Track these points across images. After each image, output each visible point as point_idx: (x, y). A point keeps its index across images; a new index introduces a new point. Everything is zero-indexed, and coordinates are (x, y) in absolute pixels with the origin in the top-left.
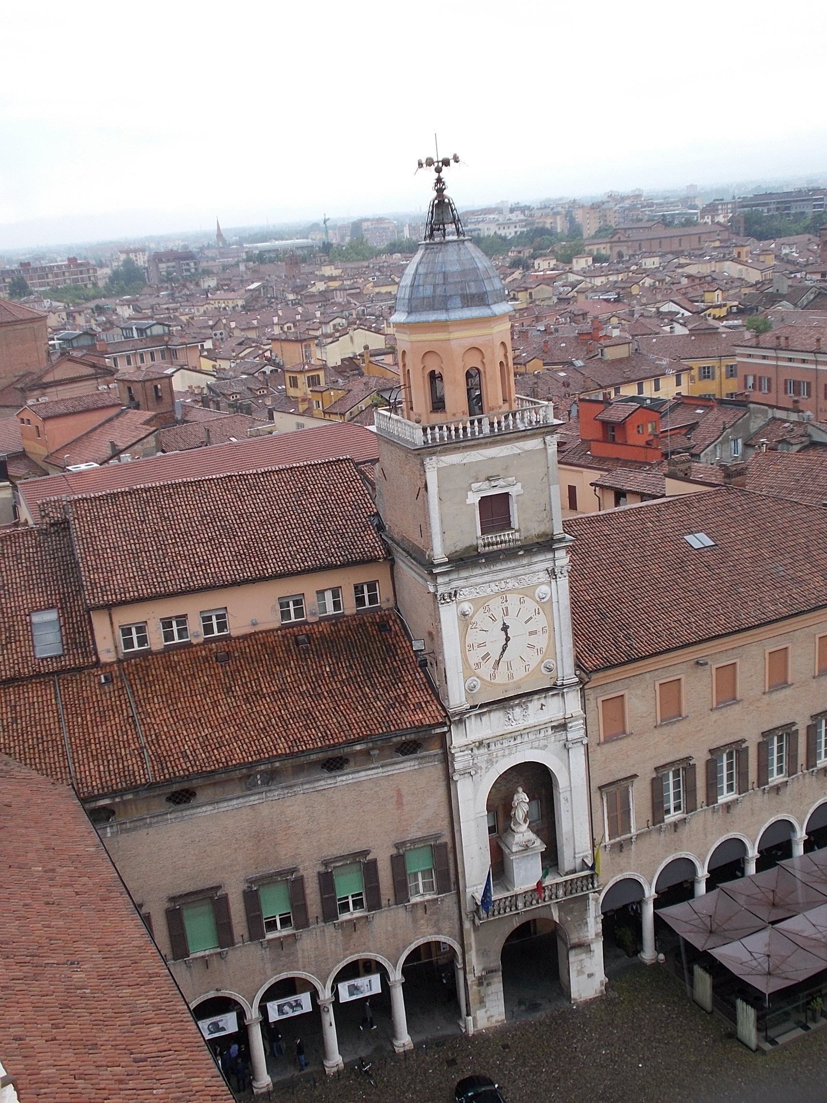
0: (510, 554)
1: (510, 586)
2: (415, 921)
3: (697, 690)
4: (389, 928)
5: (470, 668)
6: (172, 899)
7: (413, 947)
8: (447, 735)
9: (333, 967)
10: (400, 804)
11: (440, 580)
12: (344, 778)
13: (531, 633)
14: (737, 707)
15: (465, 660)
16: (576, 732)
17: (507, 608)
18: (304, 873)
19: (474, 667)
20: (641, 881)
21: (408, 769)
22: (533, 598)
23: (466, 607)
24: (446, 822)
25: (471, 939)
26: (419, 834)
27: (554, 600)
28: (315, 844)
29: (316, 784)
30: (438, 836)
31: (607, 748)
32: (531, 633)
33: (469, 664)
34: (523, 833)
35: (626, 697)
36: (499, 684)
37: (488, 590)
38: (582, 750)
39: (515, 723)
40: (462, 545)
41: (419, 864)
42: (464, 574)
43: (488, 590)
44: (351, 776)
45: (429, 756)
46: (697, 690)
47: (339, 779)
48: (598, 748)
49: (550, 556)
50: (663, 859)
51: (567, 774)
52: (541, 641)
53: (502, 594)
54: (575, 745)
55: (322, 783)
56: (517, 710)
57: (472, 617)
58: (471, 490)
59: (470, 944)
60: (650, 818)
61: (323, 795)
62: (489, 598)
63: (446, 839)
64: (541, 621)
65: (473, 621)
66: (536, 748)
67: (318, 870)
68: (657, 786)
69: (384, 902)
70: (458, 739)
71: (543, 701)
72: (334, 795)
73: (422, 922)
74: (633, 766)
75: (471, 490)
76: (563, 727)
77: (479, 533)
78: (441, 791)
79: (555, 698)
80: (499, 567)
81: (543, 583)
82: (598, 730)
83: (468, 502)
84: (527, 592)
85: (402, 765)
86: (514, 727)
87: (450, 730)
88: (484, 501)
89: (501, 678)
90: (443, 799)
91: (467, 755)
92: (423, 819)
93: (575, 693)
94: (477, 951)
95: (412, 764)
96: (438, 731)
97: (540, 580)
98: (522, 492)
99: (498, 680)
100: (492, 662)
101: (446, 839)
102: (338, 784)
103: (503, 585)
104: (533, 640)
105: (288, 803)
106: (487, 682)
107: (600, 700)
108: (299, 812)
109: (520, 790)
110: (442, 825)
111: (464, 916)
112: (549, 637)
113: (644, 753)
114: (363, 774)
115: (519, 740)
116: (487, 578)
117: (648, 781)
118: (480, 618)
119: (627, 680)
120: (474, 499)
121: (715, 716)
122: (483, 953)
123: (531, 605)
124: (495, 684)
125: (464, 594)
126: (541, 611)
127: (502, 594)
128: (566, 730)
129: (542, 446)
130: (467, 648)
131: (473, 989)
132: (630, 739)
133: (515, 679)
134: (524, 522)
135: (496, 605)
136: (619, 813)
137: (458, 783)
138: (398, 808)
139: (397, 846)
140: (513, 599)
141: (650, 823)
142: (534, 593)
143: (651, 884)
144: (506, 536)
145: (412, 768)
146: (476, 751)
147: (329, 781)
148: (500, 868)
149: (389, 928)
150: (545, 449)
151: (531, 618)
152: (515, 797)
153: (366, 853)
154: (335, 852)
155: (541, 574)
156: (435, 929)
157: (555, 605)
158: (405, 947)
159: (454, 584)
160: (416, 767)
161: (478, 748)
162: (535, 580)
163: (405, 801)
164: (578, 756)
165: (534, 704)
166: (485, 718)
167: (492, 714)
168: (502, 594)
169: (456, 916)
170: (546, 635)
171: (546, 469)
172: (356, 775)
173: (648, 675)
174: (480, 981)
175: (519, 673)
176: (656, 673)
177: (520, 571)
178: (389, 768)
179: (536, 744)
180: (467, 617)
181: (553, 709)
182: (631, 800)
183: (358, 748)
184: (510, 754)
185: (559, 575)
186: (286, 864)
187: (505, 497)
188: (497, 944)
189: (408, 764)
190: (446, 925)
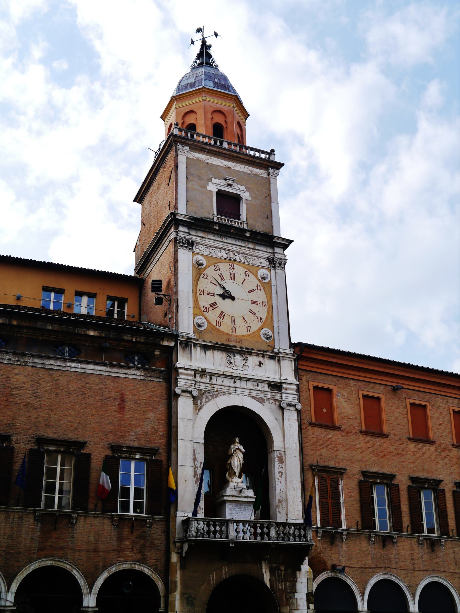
0: (239, 234)
1: (238, 258)
2: (120, 539)
3: (395, 415)
4: (92, 538)
5: (200, 308)
7: (113, 569)
8: (175, 350)
9: (24, 566)
10: (121, 408)
11: (181, 228)
12: (73, 365)
13: (253, 302)
14: (431, 448)
15: (196, 301)
16: (289, 396)
17: (234, 274)
18: (16, 446)
19: (203, 309)
20: (354, 587)
21: (134, 377)
22: (256, 276)
24: (163, 441)
26: (136, 444)
27: (273, 283)
28: (33, 420)
29: (47, 362)
30: (154, 451)
31: (317, 431)
32: (253, 302)
33: (198, 304)
34: (238, 486)
35: (334, 392)
36: (224, 333)
37: (220, 254)
38: (295, 416)
39: (235, 368)
40: (200, 215)
41: (133, 475)
42: (201, 234)
43: (220, 254)
44: (80, 365)
45: (155, 370)
46: (395, 415)
47: (69, 364)
48: (310, 428)
49: (270, 250)
51: (281, 435)
54: (288, 408)
55: (52, 362)
56: (238, 359)
57: (205, 269)
58: (211, 181)
59: (175, 582)
60: (360, 522)
61: (51, 375)
62: (220, 260)
63: (162, 457)
64: (260, 296)
65: (205, 272)
66: (253, 397)
67: (30, 447)
69: (91, 506)
70: (183, 360)
71: (261, 359)
72: (61, 379)
73: (127, 543)
74: (342, 460)
75: (211, 181)
76: (276, 386)
77: (215, 213)
78: (162, 409)
79: (272, 362)
80: (229, 241)
81: (263, 267)
83: (208, 188)
84: (251, 269)
85: (129, 371)
87: (176, 345)
88: (220, 194)
89: (225, 327)
90: (163, 418)
91: (190, 375)
92: (143, 428)
93: (289, 362)
94: (182, 594)
95: (138, 373)
96: (166, 343)
97: (261, 265)
98: (250, 199)
99: (222, 328)
100: (218, 311)
101: (162, 457)
102: (66, 369)
103: (231, 255)
104: (254, 308)
105: (17, 372)
106: (213, 325)
107: (311, 384)
108: (24, 383)
109: (237, 440)
110: (159, 442)
111: (171, 545)
112: (268, 312)
114: (91, 367)
115: (238, 384)
116: (220, 245)
117: (356, 482)
119: (334, 379)
120: (213, 187)
121: (412, 446)
123: (253, 282)
124: (220, 331)
125: (199, 249)
126: (262, 288)
127: (232, 261)
128: (281, 390)
129: (265, 175)
130: (198, 292)
132: (338, 433)
133: (237, 334)
136: (330, 501)
137: (181, 400)
138: (119, 412)
139: (114, 448)
141: (360, 526)
142: (257, 272)
143: (363, 596)
145: (138, 377)
146: (198, 378)
147: (59, 363)
148: (213, 502)
149: (92, 538)
150: (268, 179)
151: (253, 290)
152: (232, 446)
153: (83, 445)
154: (49, 434)
155: (263, 261)
156: (139, 556)
157: (273, 288)
158: (105, 567)
159: (194, 238)
160: (142, 378)
161: (201, 377)
162: (258, 262)
163: (127, 406)
165: (253, 360)
166: (209, 353)
167: (216, 352)
169: (163, 548)
170: (266, 309)
171: (269, 192)
172: (85, 366)
173: (352, 382)
175: (241, 331)
176: (359, 384)
177: (246, 251)
178: (117, 370)
179: (254, 393)
180: (200, 267)
181: (270, 371)
182: (341, 494)
183: (92, 333)
184: (230, 393)
185: (277, 265)
187: (237, 199)
188: (203, 594)
189: (135, 372)
190: (152, 555)
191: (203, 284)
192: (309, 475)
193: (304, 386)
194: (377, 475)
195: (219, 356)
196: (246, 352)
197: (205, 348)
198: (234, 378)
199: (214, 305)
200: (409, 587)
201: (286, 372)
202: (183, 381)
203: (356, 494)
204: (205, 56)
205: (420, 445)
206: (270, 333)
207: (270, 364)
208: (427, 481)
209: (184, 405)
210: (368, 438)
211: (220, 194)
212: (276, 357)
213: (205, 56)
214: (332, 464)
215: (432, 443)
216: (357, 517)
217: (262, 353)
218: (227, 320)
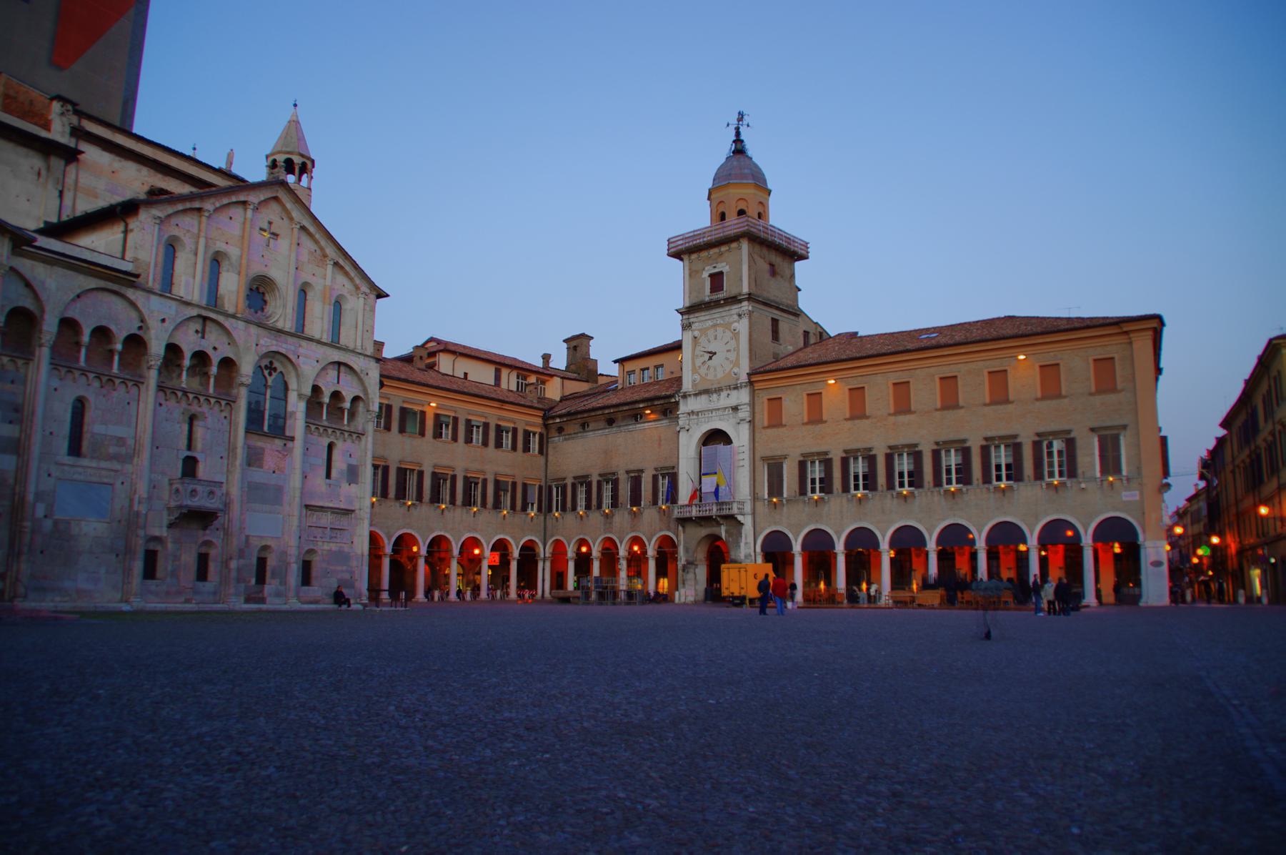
6: (575, 478)
14: (865, 421)
15: (693, 363)
16: (744, 413)
20: (791, 536)
23: (696, 333)
25: (682, 537)
31: (769, 431)
50: (807, 525)
52: (732, 356)
53: (715, 326)
56: (715, 395)
62: (707, 329)
64: (733, 344)
68: (802, 466)
70: (684, 408)
76: (735, 409)
82: (763, 418)
84: (727, 326)
86: (712, 406)
88: (711, 276)
89: (710, 377)
104: (729, 355)
113: (794, 442)
118: (703, 340)
120: (705, 275)
121: (849, 424)
122: (687, 550)
123: (729, 334)
131: (680, 572)
134: (728, 289)
135: (711, 333)
140: (720, 330)
144: (721, 295)
164: (745, 430)
165: (724, 394)
168: (715, 326)
174: (684, 568)
175: (720, 375)
186: (614, 470)
191: (699, 350)
192: (759, 463)
193: (758, 401)
194: (812, 454)
195: (704, 397)
196: (719, 390)
197: (696, 395)
198: (711, 411)
199: (704, 363)
200: (836, 532)
201: (743, 396)
202: (681, 422)
203: (796, 471)
204: (738, 140)
205: (857, 422)
206: (736, 370)
207: (734, 393)
208: (858, 450)
209: (683, 437)
210: (810, 427)
211: (711, 276)
212: (736, 388)
213: (738, 140)
214: (779, 453)
215: (867, 418)
216: (796, 487)
217: (729, 387)
218: (712, 370)
